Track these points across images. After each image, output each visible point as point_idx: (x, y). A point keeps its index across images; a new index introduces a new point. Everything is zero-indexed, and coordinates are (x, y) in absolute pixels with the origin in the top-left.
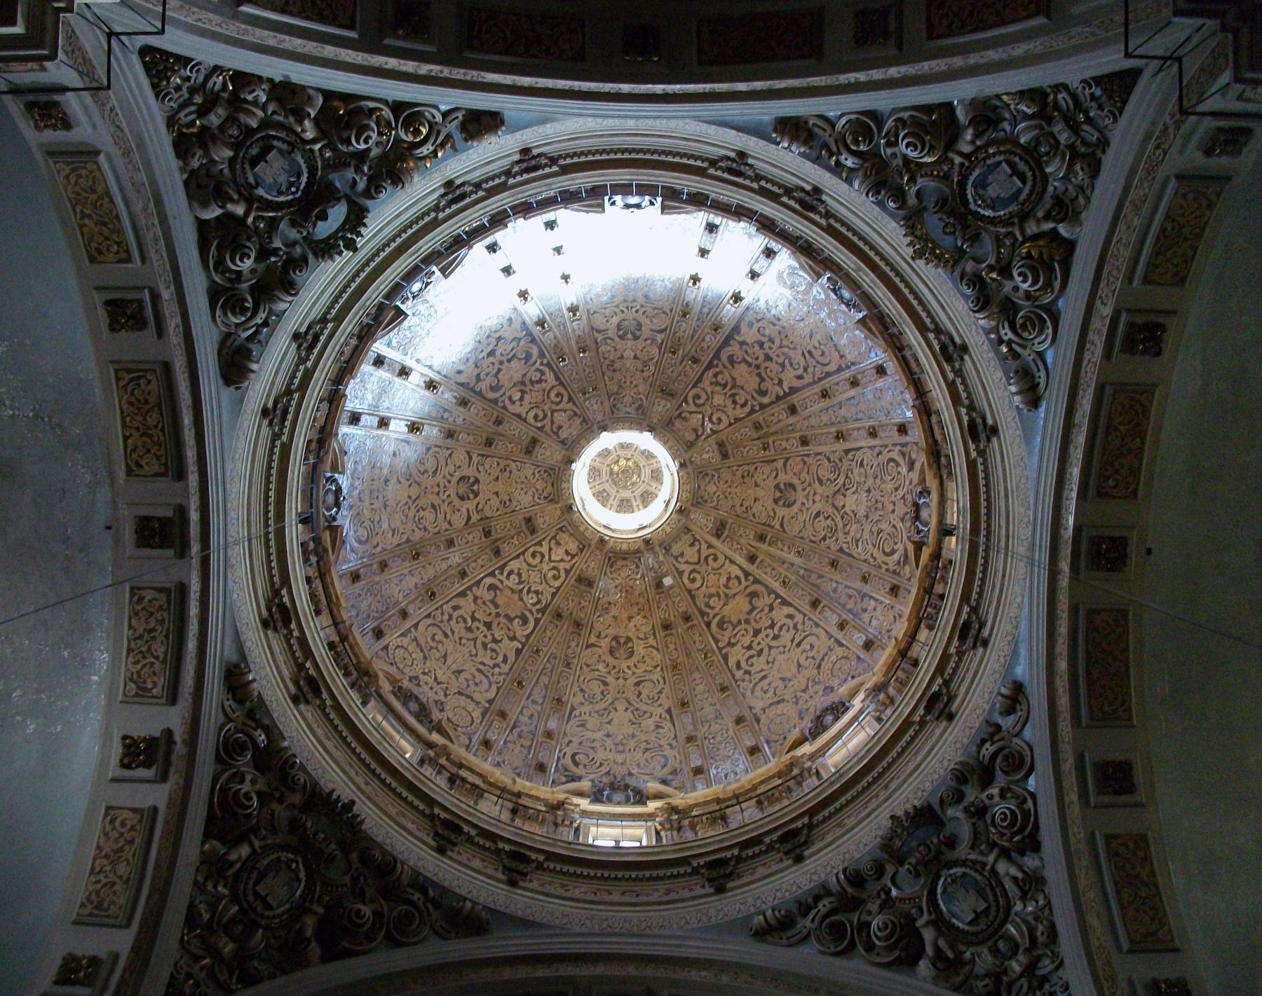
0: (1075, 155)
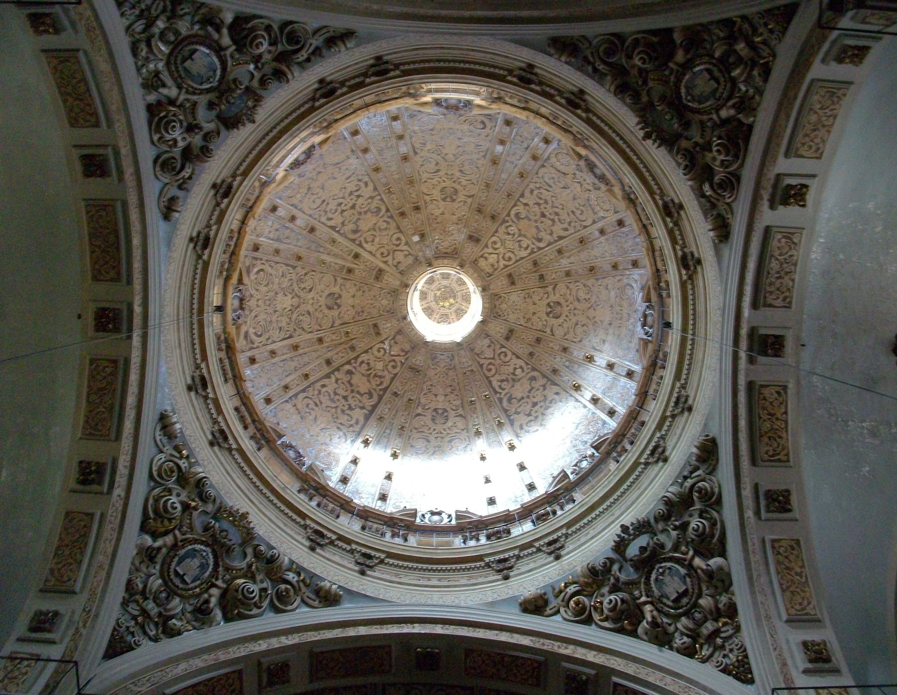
0: (143, 593)
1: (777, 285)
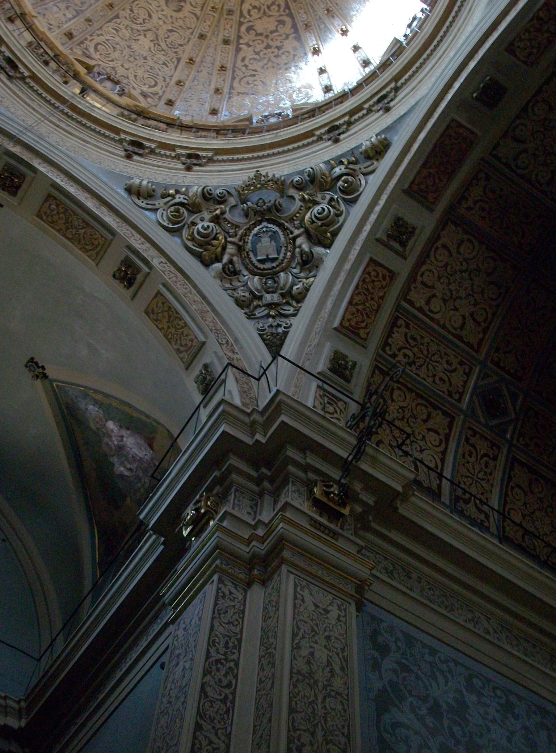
0: (255, 297)
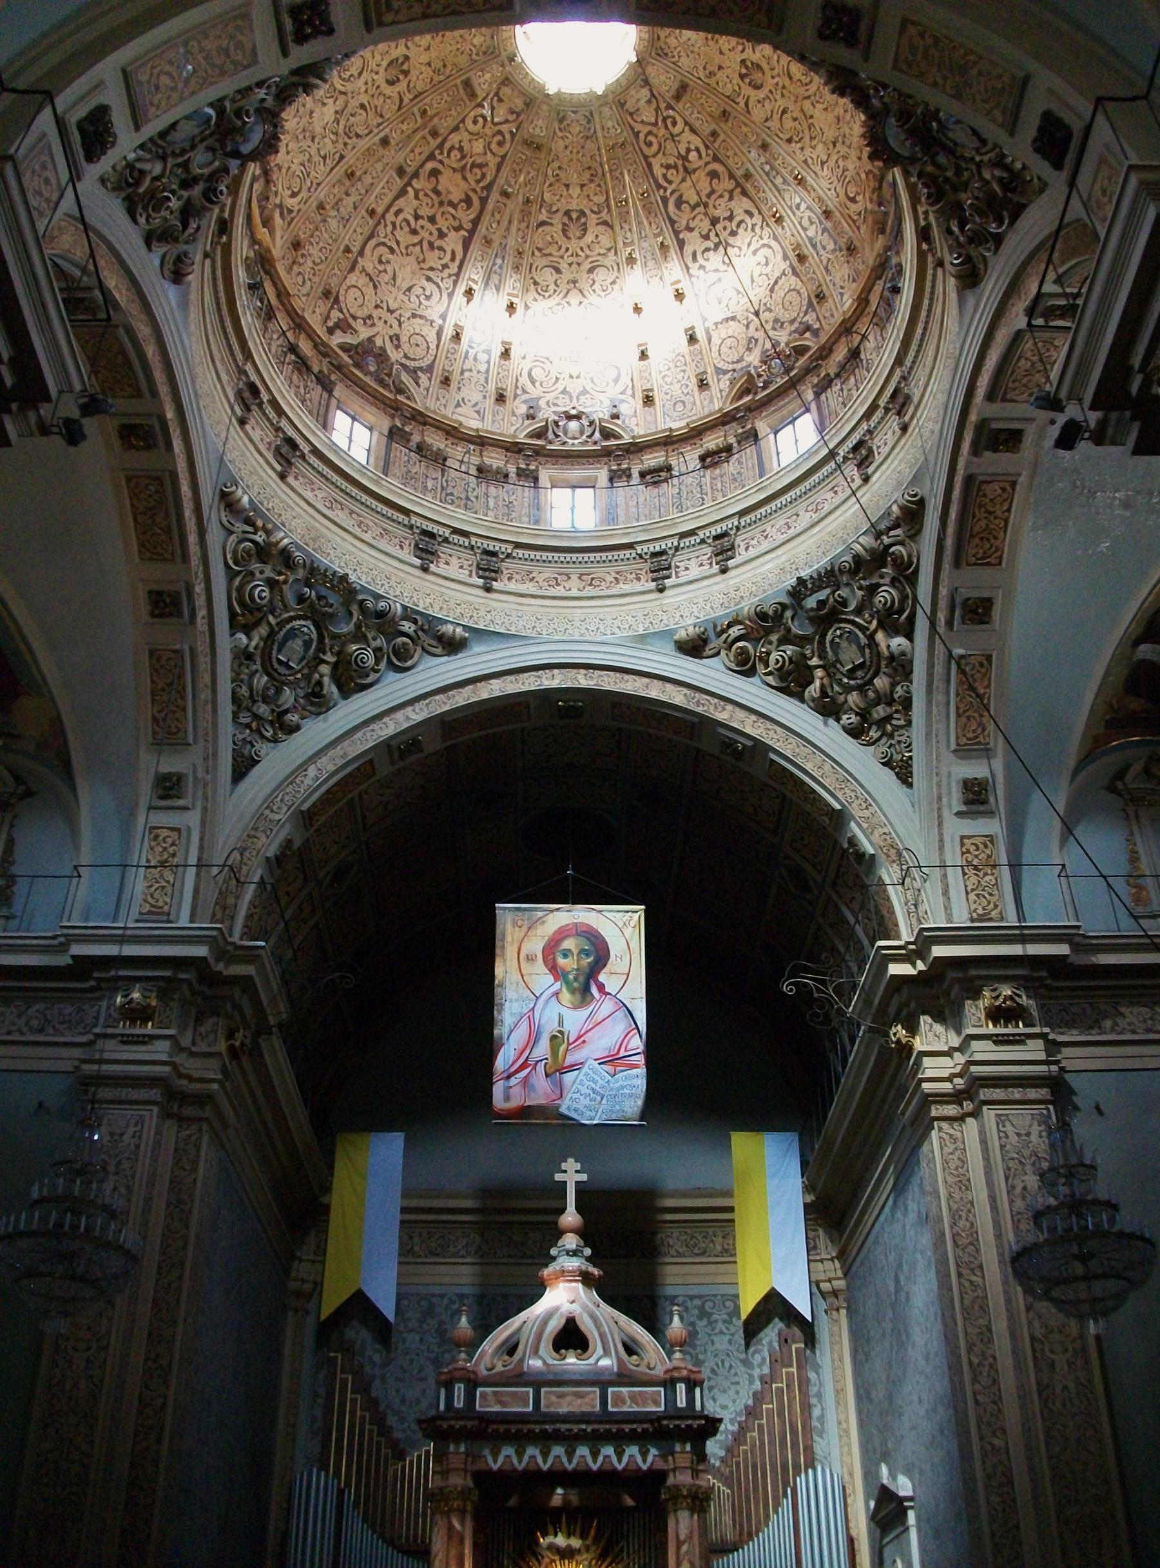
1: (1025, 380)
